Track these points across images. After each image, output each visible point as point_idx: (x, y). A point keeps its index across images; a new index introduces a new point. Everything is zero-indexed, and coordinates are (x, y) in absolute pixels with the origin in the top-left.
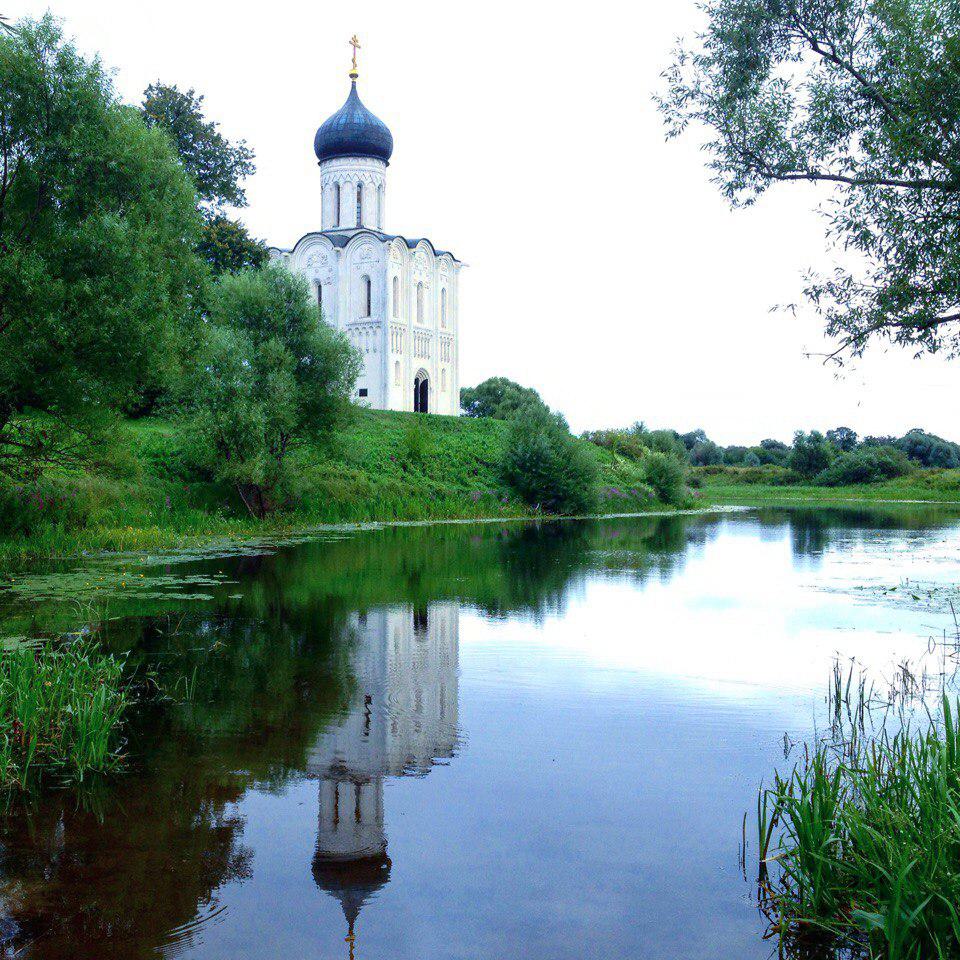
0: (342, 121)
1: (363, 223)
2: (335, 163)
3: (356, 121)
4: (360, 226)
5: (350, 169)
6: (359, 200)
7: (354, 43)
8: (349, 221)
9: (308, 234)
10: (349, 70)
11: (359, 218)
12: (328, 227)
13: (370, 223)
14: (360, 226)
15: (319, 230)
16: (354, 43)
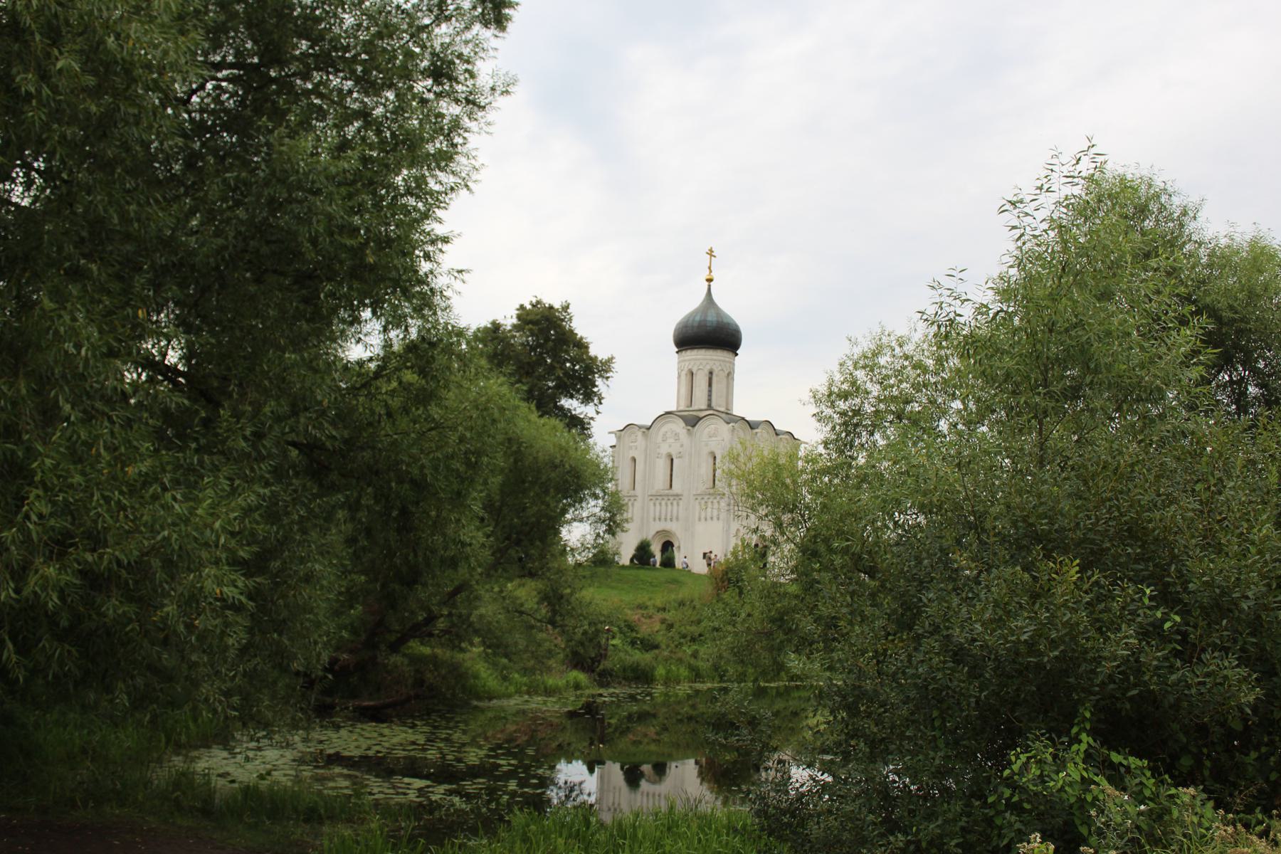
0: (698, 318)
1: (713, 404)
2: (689, 352)
3: (709, 318)
4: (710, 407)
5: (703, 358)
6: (710, 385)
7: (711, 253)
8: (700, 402)
9: (668, 413)
10: (706, 275)
11: (710, 400)
12: (681, 408)
13: (718, 403)
14: (710, 407)
15: (674, 409)
16: (711, 253)
